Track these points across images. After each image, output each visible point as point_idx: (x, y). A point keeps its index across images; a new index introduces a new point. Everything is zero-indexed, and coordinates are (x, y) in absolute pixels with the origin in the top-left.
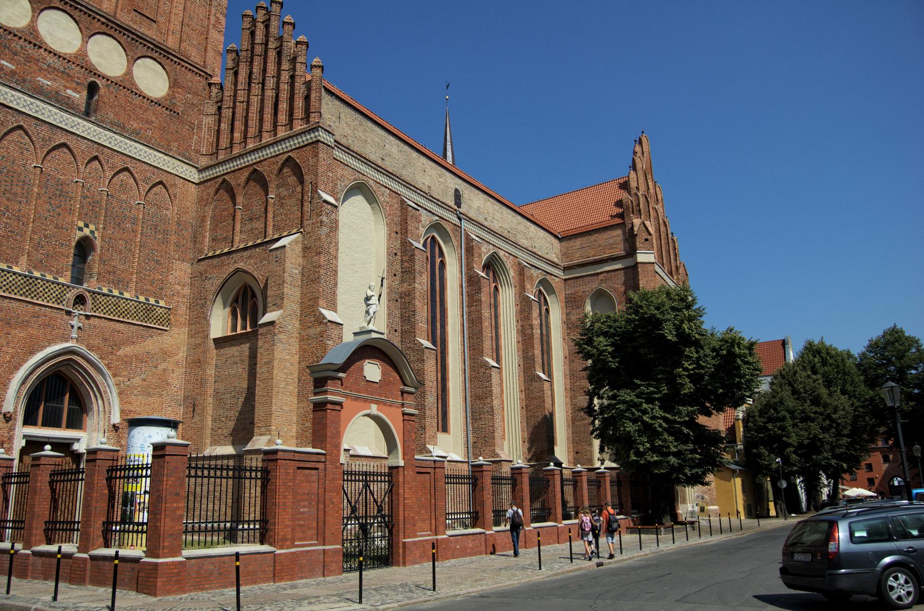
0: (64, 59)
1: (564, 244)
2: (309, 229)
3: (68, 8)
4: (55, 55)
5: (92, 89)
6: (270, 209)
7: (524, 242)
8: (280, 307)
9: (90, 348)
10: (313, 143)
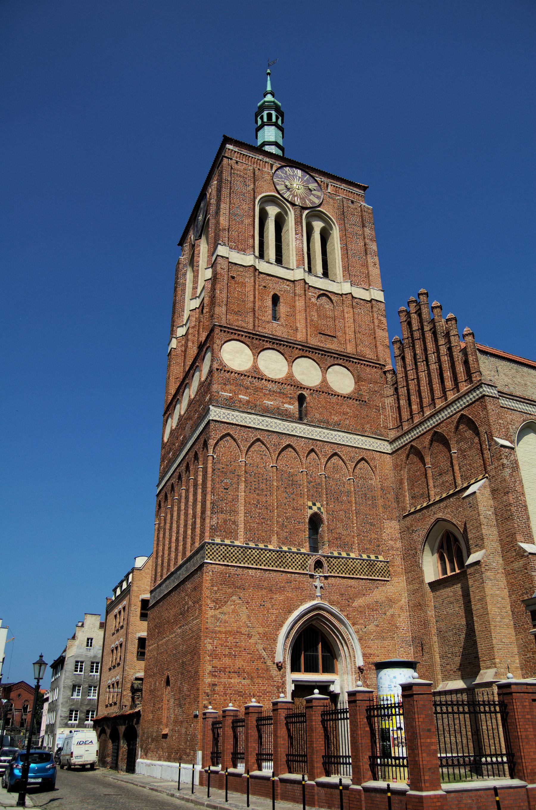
0: (279, 383)
2: (493, 473)
3: (275, 346)
4: (272, 381)
5: (301, 399)
6: (455, 462)
8: (481, 547)
9: (332, 603)
10: (480, 398)
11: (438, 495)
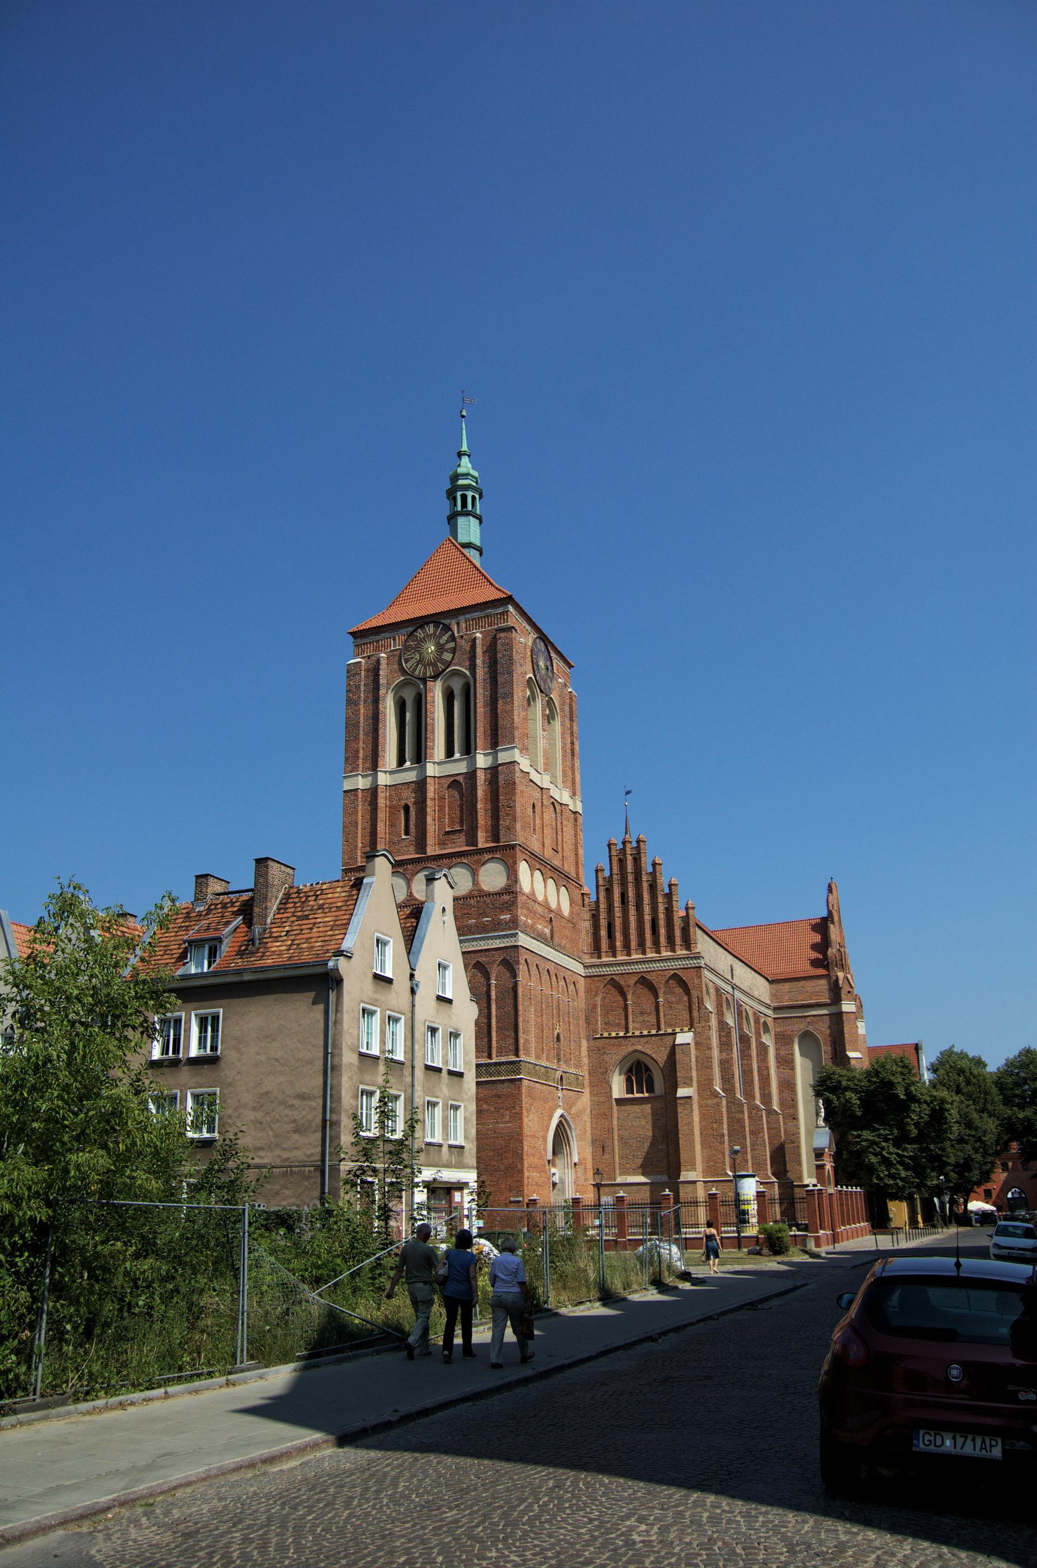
1: (773, 986)
2: (699, 1030)
6: (661, 1009)
7: (756, 994)
11: (637, 1029)
